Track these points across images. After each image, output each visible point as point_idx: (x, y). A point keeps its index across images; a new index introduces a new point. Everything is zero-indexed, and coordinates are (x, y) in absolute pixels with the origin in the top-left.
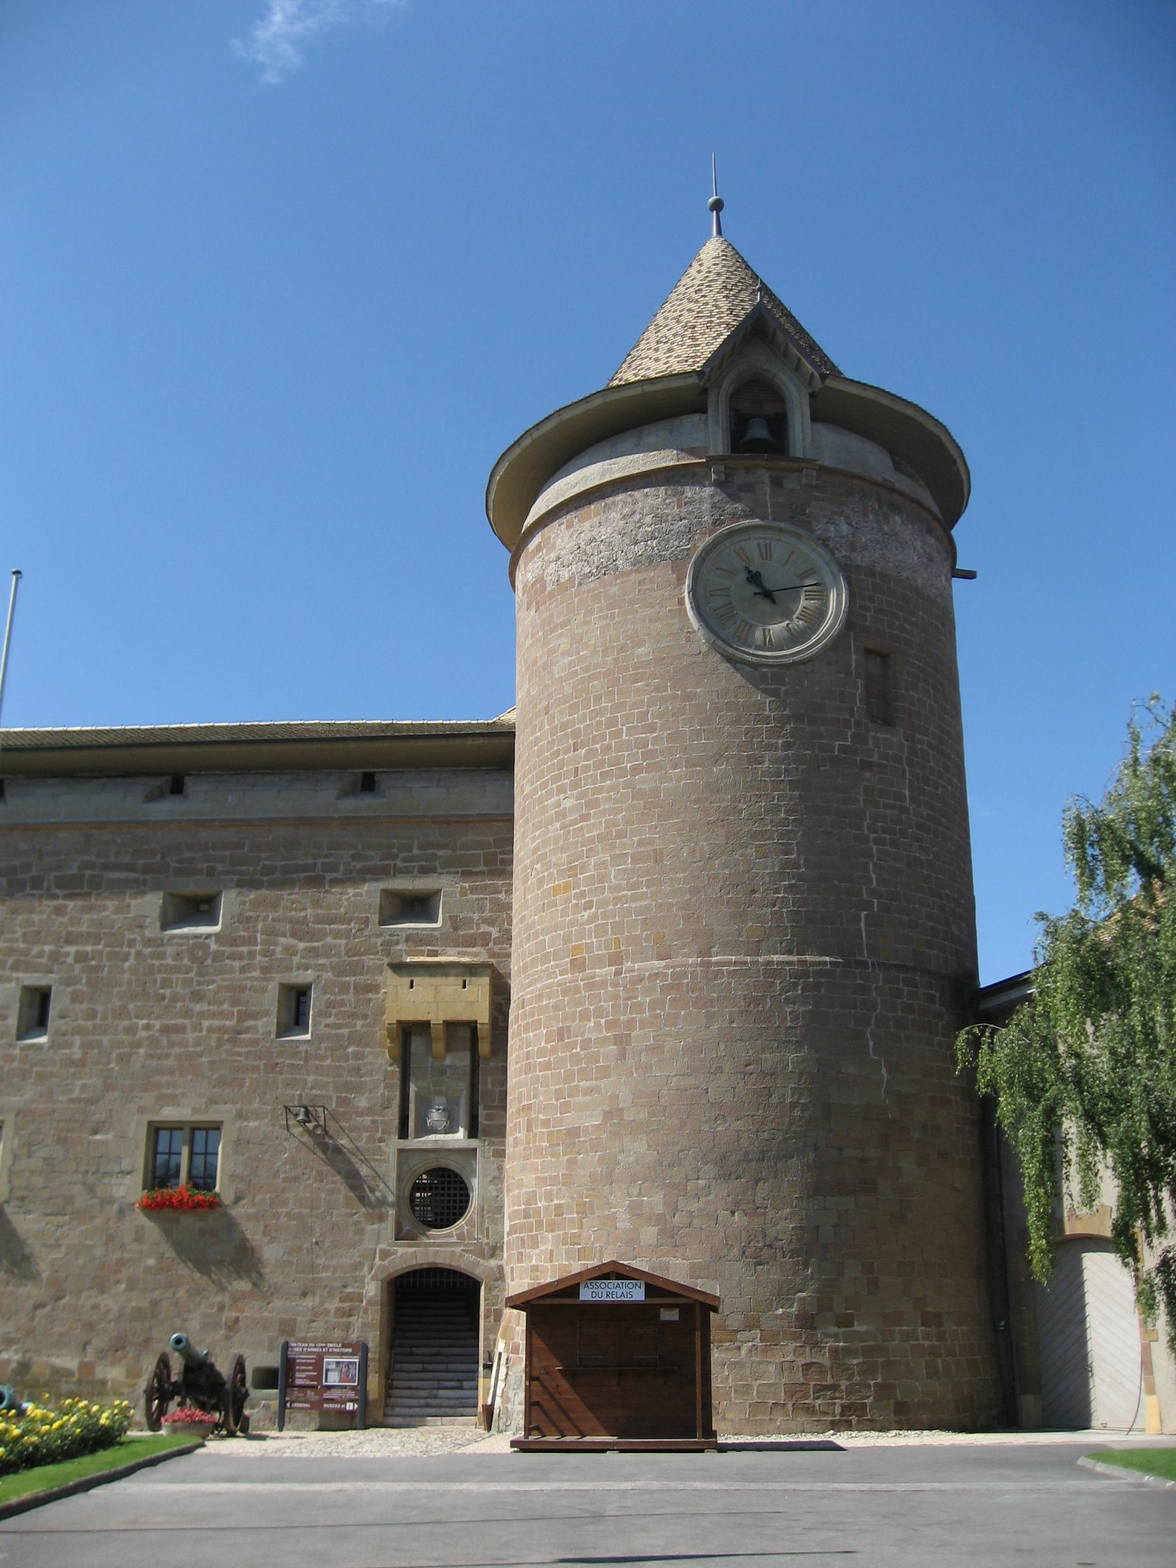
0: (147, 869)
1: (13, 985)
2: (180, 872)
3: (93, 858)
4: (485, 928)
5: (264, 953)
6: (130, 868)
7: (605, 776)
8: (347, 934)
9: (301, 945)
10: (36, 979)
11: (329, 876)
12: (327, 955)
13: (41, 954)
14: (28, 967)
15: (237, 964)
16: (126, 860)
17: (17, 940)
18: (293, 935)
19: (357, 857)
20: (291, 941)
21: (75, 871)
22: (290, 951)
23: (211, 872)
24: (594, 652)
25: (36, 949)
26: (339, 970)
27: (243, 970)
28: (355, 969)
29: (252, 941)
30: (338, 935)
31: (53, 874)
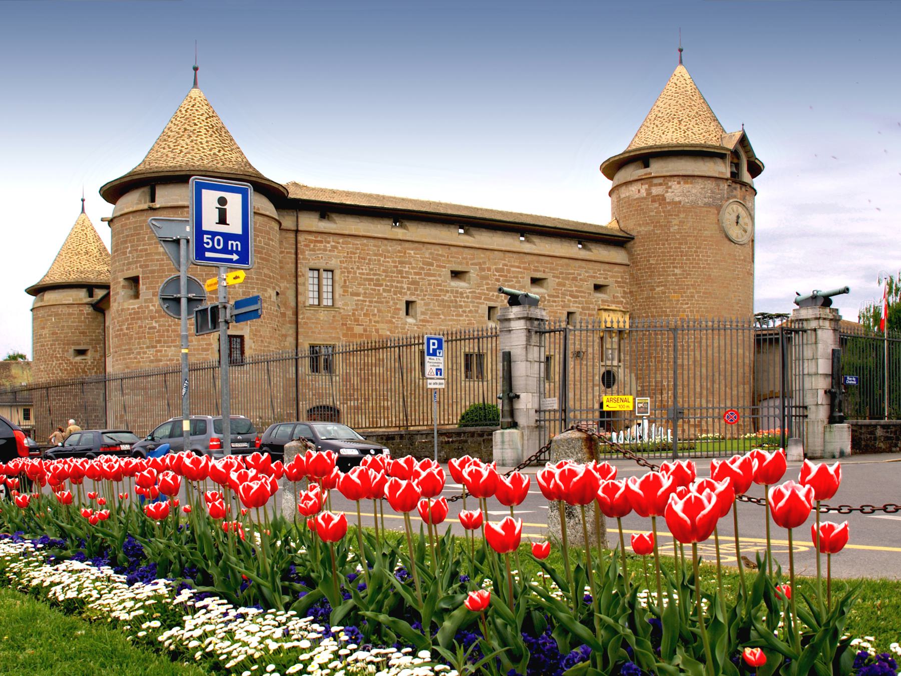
0: (524, 268)
1: (485, 306)
2: (535, 270)
3: (506, 262)
4: (622, 299)
5: (562, 301)
6: (519, 267)
7: (693, 267)
8: (584, 297)
9: (573, 300)
10: (492, 304)
11: (579, 277)
12: (579, 303)
13: (493, 295)
14: (489, 300)
15: (554, 304)
16: (517, 264)
17: (484, 290)
18: (571, 296)
19: (586, 272)
20: (570, 298)
21: (501, 266)
22: (569, 301)
23: (544, 272)
24: (690, 228)
25: (491, 293)
26: (583, 308)
27: (556, 306)
28: (589, 309)
29: (558, 297)
30: (581, 297)
31: (494, 267)
